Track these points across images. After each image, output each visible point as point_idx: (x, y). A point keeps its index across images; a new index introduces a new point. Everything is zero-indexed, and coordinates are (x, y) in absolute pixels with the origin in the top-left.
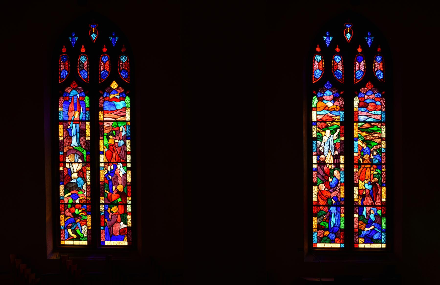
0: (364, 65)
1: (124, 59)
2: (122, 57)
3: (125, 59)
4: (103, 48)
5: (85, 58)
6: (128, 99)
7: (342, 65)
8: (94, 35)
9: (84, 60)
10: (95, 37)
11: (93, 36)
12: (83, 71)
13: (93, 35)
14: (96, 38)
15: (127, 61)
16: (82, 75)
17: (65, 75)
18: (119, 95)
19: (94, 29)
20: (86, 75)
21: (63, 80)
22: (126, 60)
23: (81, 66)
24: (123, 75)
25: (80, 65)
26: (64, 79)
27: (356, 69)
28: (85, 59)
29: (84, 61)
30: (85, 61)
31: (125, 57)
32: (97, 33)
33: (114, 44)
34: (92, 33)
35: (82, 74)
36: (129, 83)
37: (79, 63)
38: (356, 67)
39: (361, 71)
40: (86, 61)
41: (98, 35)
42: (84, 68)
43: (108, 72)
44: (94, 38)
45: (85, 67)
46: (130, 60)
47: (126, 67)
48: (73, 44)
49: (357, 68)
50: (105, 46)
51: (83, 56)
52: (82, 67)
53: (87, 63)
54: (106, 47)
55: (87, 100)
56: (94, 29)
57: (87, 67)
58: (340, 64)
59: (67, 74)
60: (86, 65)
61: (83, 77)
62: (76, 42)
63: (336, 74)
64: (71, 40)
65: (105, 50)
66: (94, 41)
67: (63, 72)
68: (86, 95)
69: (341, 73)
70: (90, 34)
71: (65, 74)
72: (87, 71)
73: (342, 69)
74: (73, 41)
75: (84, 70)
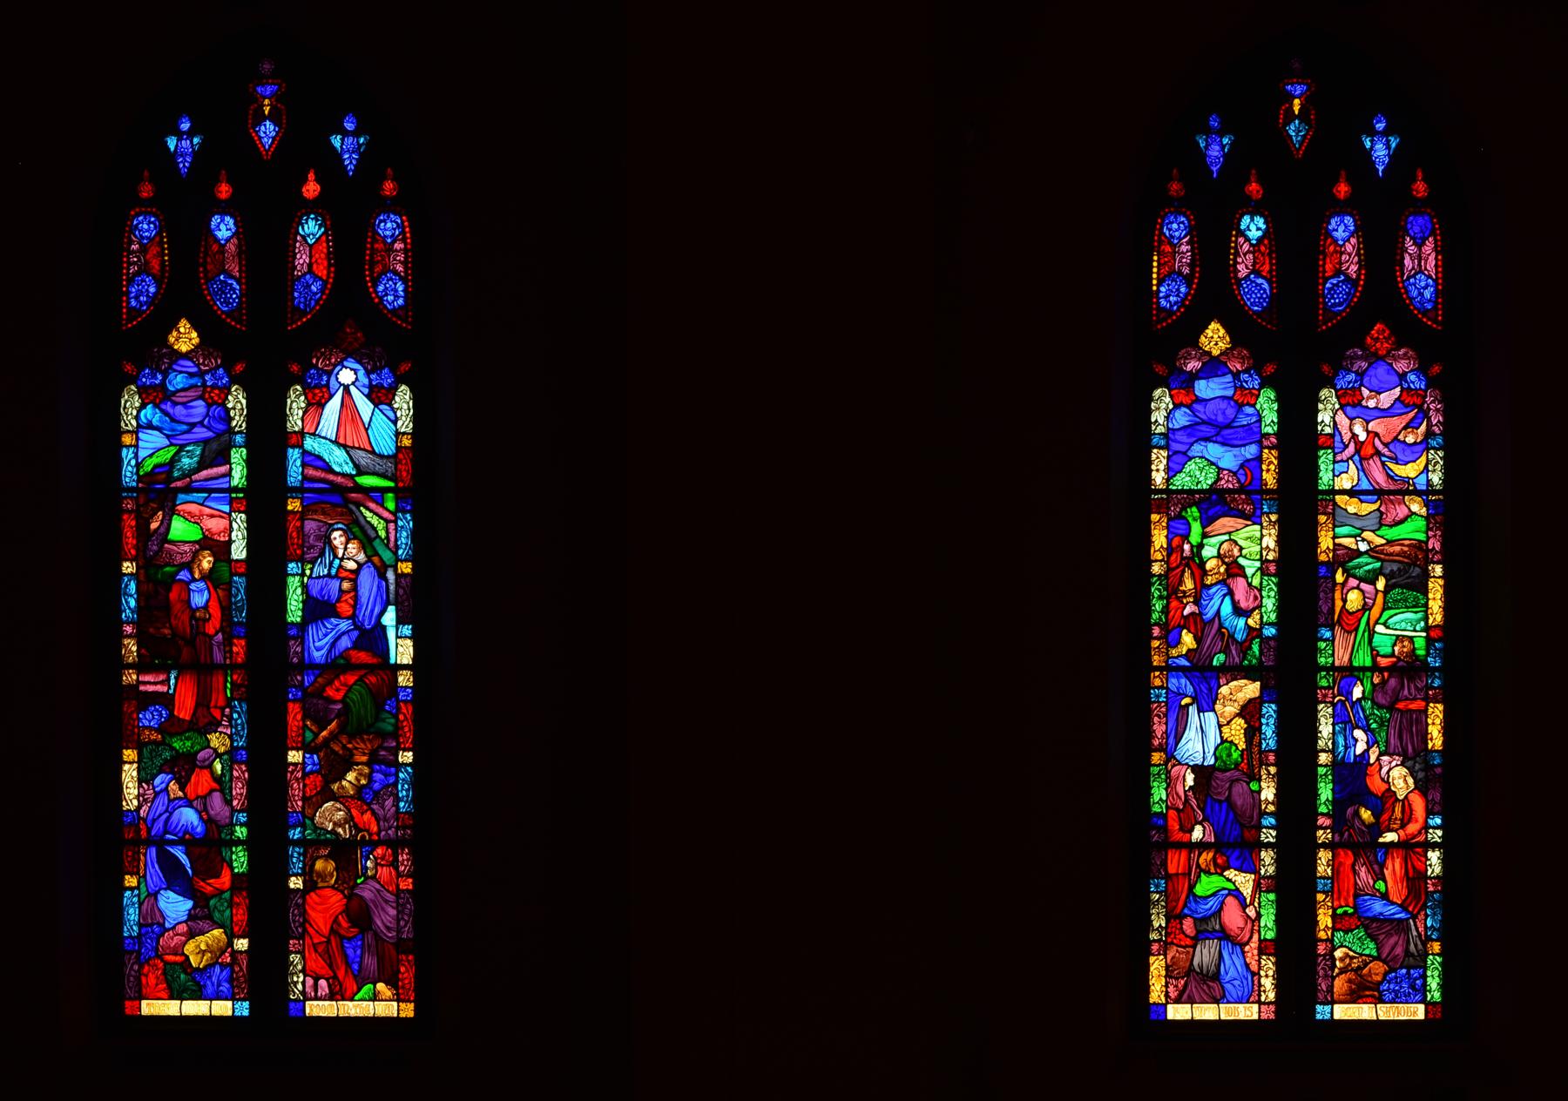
0: (1358, 254)
2: (381, 221)
3: (394, 229)
4: (305, 180)
6: (403, 399)
7: (1269, 254)
10: (273, 134)
11: (265, 133)
13: (263, 128)
14: (278, 138)
24: (387, 295)
27: (1324, 271)
33: (350, 161)
34: (261, 118)
36: (409, 327)
38: (1328, 260)
39: (1346, 275)
44: (267, 141)
50: (311, 176)
58: (1263, 248)
59: (155, 294)
63: (1244, 289)
65: (311, 189)
69: (1266, 286)
73: (1270, 271)
74: (182, 156)
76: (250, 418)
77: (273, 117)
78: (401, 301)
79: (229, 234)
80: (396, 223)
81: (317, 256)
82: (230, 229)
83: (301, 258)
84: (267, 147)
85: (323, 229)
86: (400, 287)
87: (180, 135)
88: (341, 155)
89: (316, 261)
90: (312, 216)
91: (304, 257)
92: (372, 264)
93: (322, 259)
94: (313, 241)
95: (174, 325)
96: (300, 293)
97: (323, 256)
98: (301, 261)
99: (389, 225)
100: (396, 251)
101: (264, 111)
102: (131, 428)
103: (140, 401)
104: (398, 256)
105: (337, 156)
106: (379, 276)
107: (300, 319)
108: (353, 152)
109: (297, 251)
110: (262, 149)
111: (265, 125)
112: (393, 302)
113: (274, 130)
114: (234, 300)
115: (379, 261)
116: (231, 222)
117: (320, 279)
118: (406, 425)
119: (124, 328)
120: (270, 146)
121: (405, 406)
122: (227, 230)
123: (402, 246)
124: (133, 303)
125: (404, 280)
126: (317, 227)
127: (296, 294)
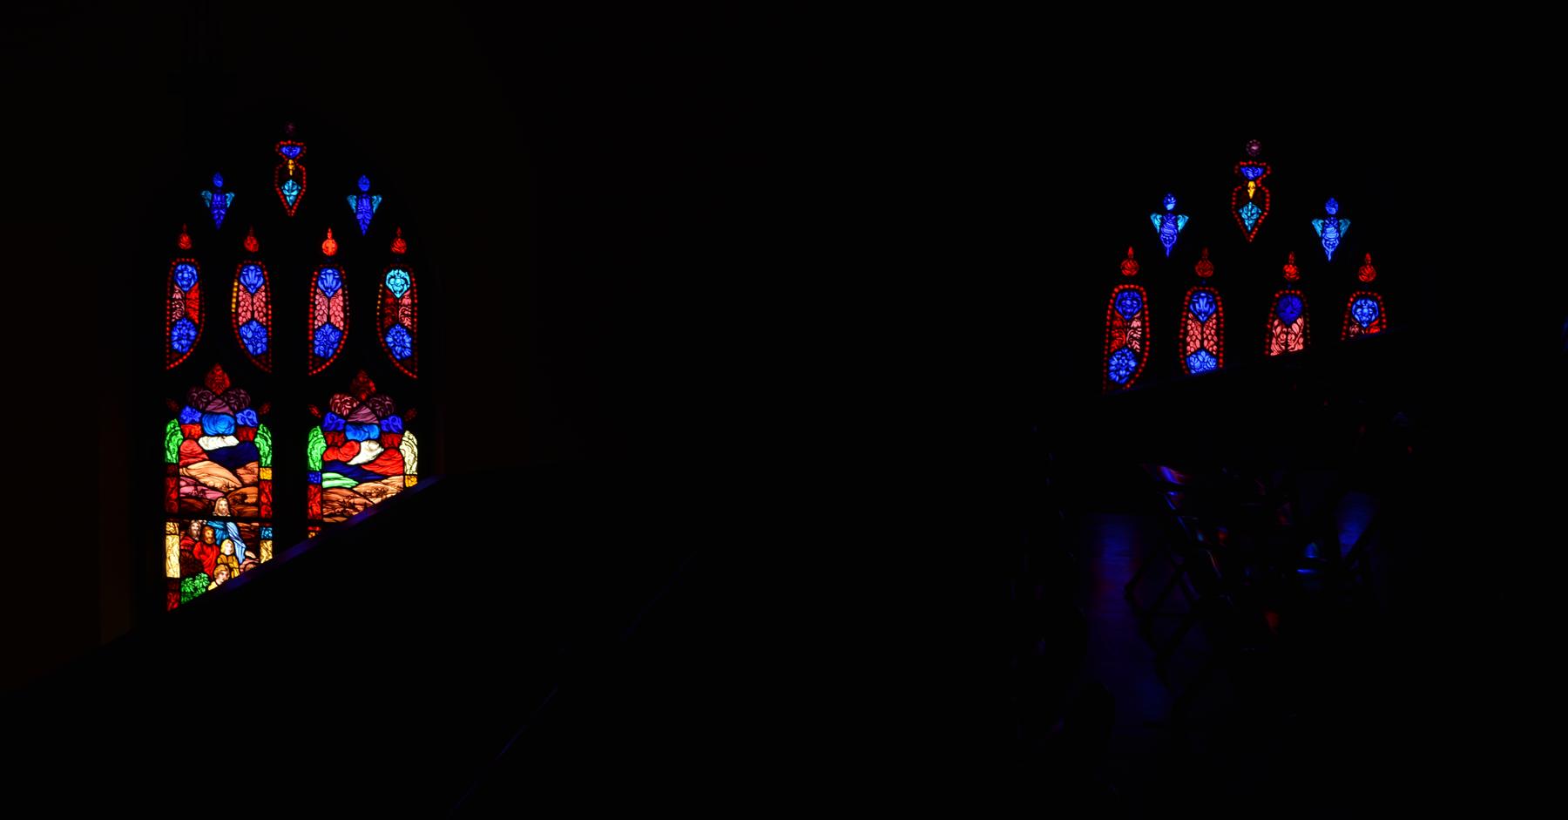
1: (398, 281)
3: (403, 285)
5: (259, 276)
9: (256, 282)
12: (251, 327)
15: (408, 293)
16: (245, 341)
17: (188, 339)
18: (379, 425)
20: (262, 342)
21: (181, 357)
22: (405, 289)
23: (244, 305)
25: (242, 303)
26: (185, 354)
28: (259, 280)
29: (255, 285)
30: (260, 287)
31: (403, 278)
35: (247, 338)
36: (415, 377)
37: (238, 296)
40: (263, 287)
42: (256, 315)
43: (342, 333)
45: (257, 309)
46: (419, 287)
47: (407, 315)
49: (1277, 347)
50: (329, 235)
51: (252, 268)
52: (248, 309)
53: (266, 297)
55: (263, 444)
57: (265, 310)
59: (196, 336)
60: (262, 304)
61: (251, 348)
62: (227, 210)
64: (211, 204)
65: (330, 246)
66: (291, 213)
67: (180, 329)
71: (188, 335)
72: (267, 327)
75: (254, 323)
77: (297, 178)
78: (407, 353)
80: (405, 280)
81: (334, 309)
85: (340, 284)
86: (408, 340)
90: (330, 271)
91: (323, 308)
92: (383, 315)
97: (340, 309)
98: (321, 313)
99: (399, 281)
100: (404, 305)
104: (406, 310)
106: (389, 328)
107: (320, 366)
109: (317, 303)
112: (402, 351)
115: (389, 314)
117: (338, 329)
120: (294, 204)
123: (409, 301)
124: (176, 346)
125: (410, 333)
126: (335, 282)
127: (317, 343)
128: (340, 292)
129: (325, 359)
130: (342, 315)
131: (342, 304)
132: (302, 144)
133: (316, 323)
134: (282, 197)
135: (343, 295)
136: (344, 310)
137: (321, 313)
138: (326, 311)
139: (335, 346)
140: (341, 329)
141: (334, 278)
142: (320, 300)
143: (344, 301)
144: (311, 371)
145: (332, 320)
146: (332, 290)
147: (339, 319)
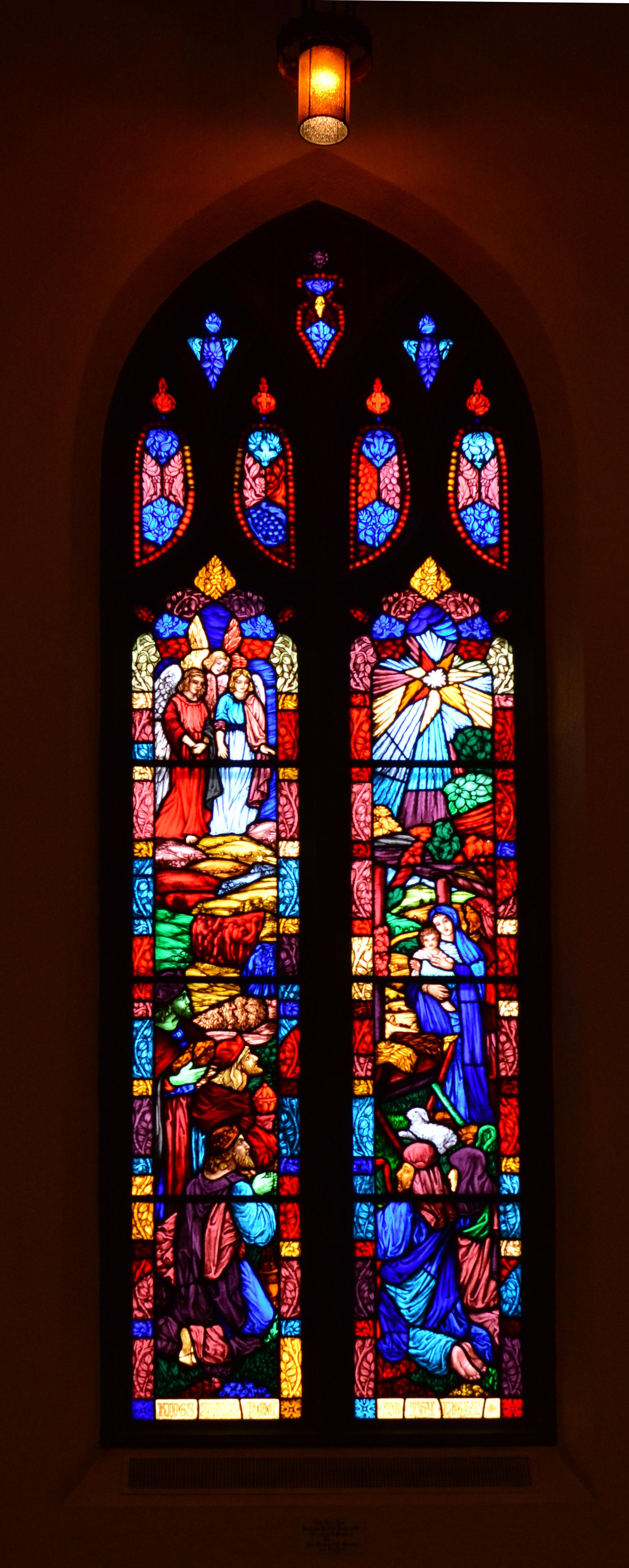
8: (321, 328)
10: (329, 337)
11: (318, 336)
19: (320, 300)
32: (338, 320)
41: (342, 328)
48: (213, 373)
54: (386, 391)
56: (320, 300)
65: (378, 402)
68: (280, 629)
70: (299, 323)
74: (209, 360)
76: (303, 675)
77: (329, 318)
79: (273, 454)
82: (275, 449)
83: (367, 482)
84: (321, 352)
85: (394, 450)
87: (207, 337)
88: (417, 364)
89: (386, 487)
91: (370, 481)
93: (393, 485)
94: (382, 461)
95: (204, 562)
96: (366, 524)
97: (394, 481)
98: (367, 487)
101: (315, 311)
102: (145, 688)
103: (158, 654)
105: (411, 367)
107: (366, 557)
108: (432, 360)
109: (361, 474)
110: (314, 356)
111: (318, 327)
113: (330, 332)
114: (280, 531)
116: (276, 441)
117: (392, 507)
118: (505, 683)
119: (137, 564)
120: (325, 351)
121: (503, 661)
122: (271, 450)
126: (387, 446)
128: (395, 459)
129: (372, 549)
130: (398, 489)
131: (397, 475)
132: (335, 277)
133: (360, 499)
134: (307, 343)
135: (399, 463)
136: (401, 481)
137: (367, 487)
138: (375, 486)
139: (389, 529)
140: (397, 506)
141: (385, 442)
142: (366, 471)
143: (400, 471)
144: (354, 563)
145: (384, 495)
146: (382, 457)
147: (394, 495)
